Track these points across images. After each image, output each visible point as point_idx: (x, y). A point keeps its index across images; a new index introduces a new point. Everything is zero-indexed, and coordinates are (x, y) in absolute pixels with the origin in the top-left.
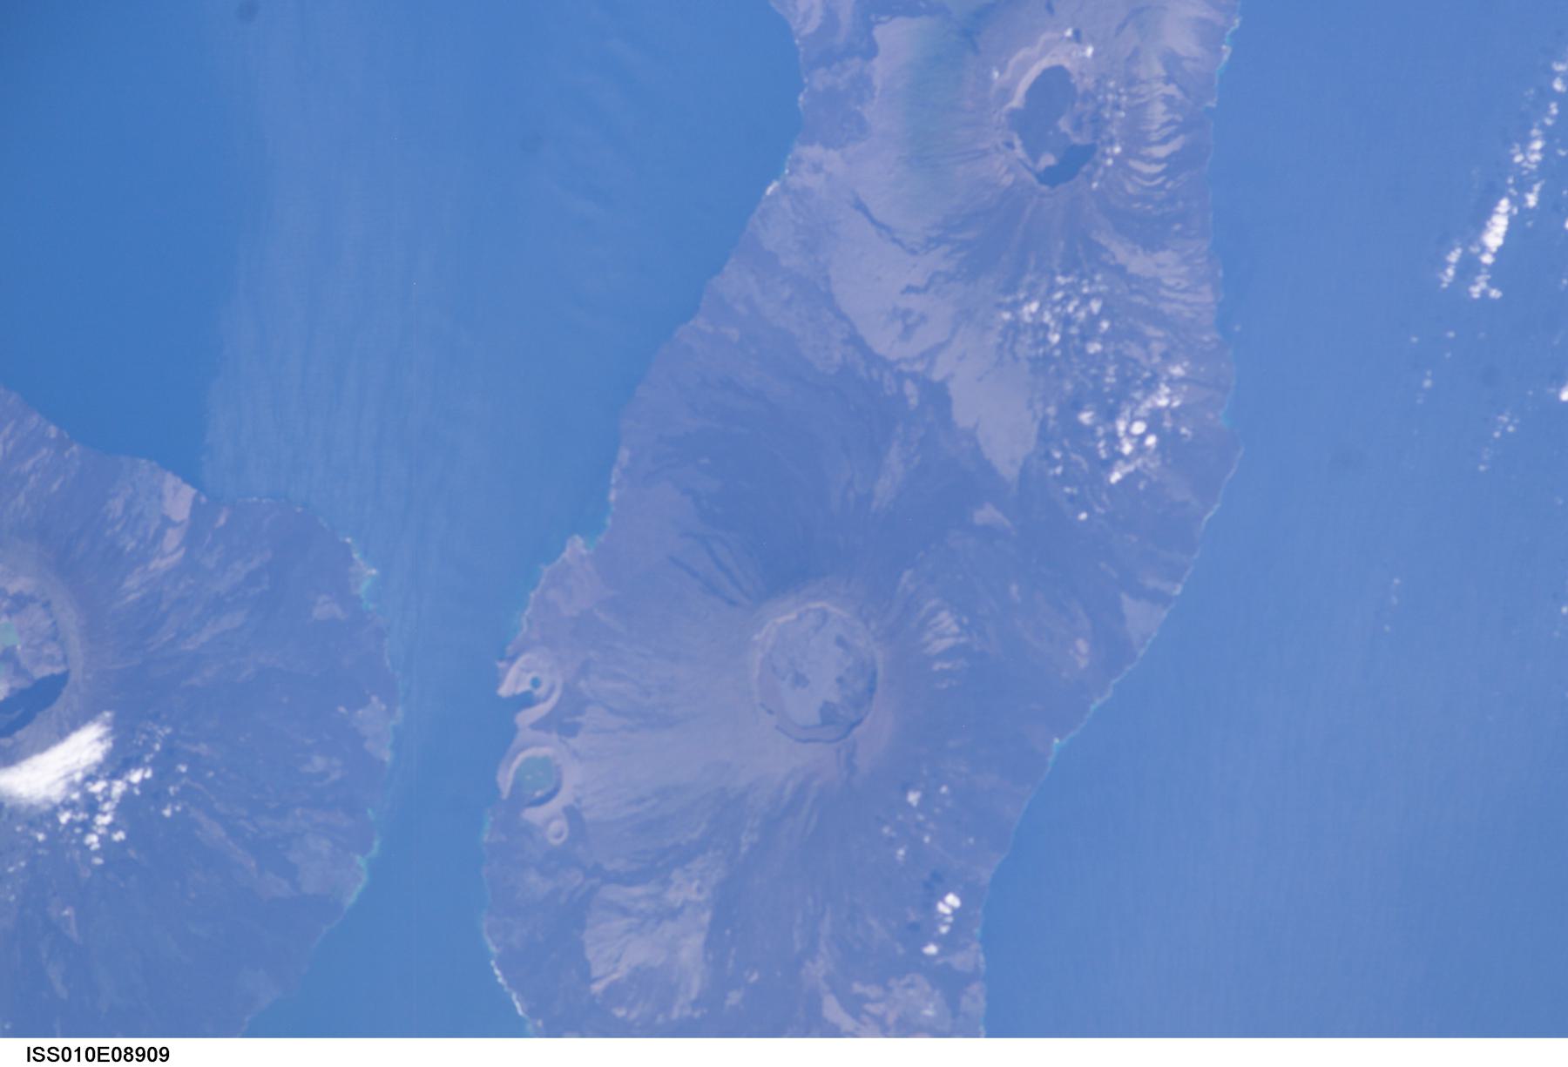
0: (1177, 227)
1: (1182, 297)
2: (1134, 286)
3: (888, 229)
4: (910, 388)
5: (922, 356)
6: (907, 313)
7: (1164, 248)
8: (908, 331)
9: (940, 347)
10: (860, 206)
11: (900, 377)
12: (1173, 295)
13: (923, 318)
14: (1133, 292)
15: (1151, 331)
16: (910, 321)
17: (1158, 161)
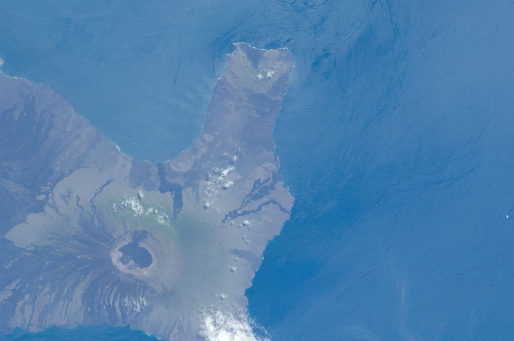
0: (89, 310)
1: (64, 310)
2: (70, 290)
3: (100, 191)
4: (42, 197)
5: (54, 202)
6: (69, 196)
7: (82, 303)
8: (63, 197)
9: (57, 209)
10: (109, 182)
11: (47, 193)
12: (65, 306)
13: (67, 203)
14: (68, 288)
15: (53, 296)
16: (67, 198)
17: (114, 303)
